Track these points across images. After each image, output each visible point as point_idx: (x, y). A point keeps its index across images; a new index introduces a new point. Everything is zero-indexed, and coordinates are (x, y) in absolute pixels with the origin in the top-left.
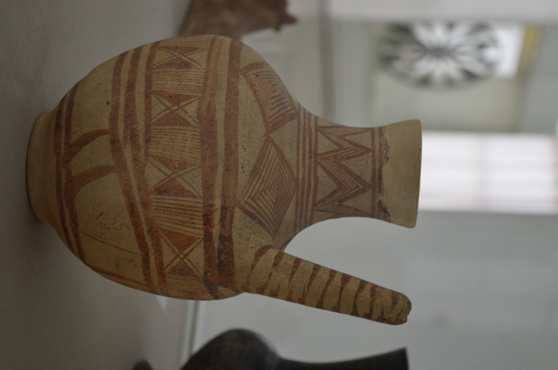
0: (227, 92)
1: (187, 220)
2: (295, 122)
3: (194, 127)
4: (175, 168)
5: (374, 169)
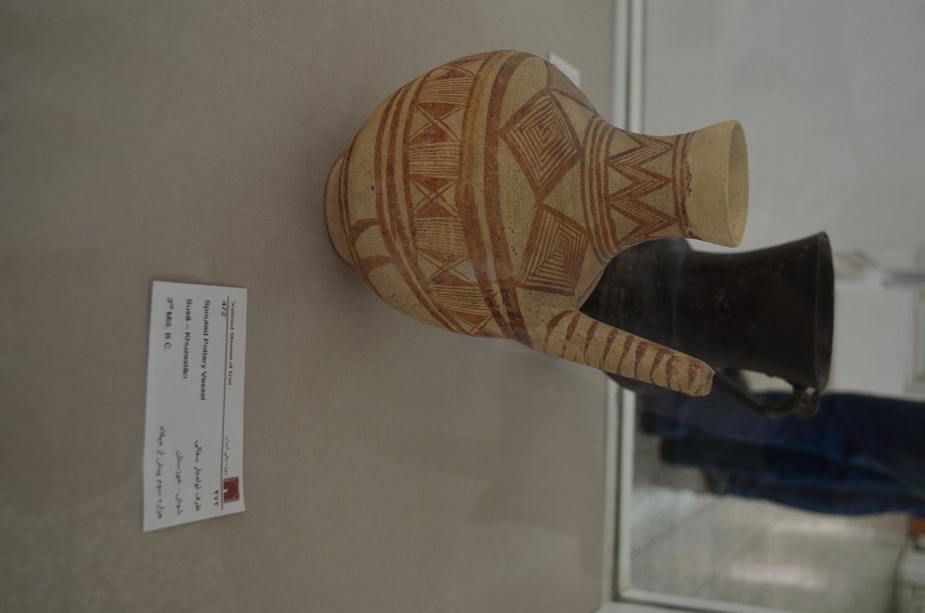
0: (485, 169)
1: (471, 304)
2: (576, 168)
4: (445, 260)
5: (676, 203)
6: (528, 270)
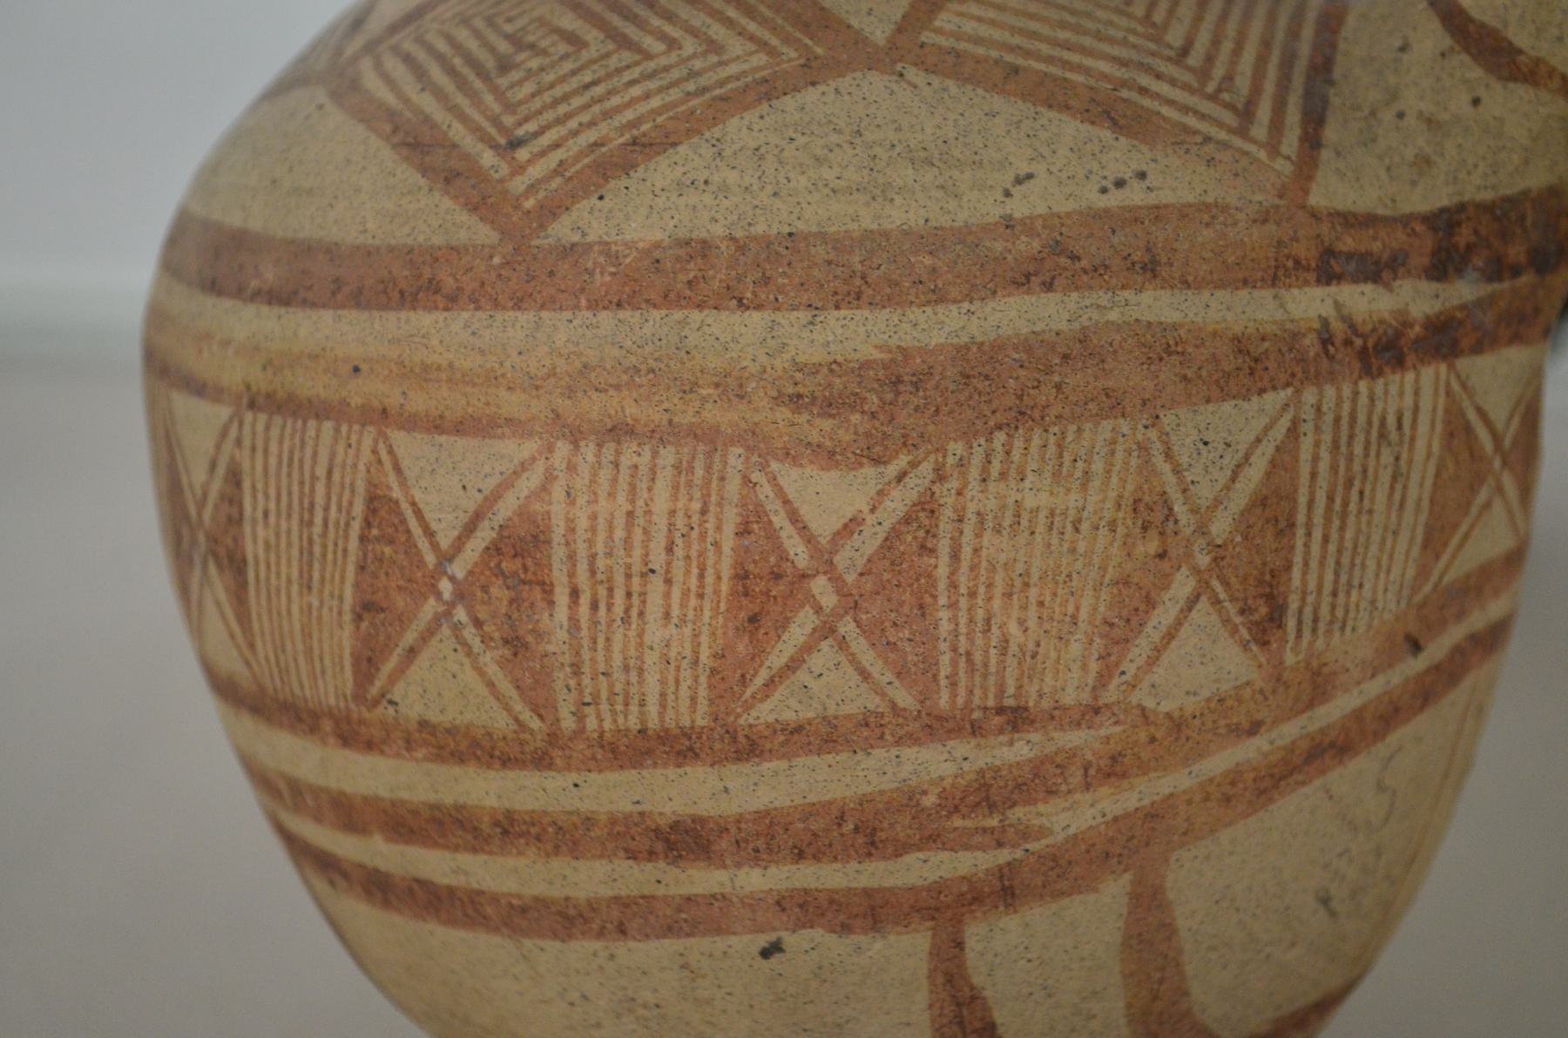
0: (700, 306)
1: (1387, 457)
3: (940, 476)
4: (1162, 556)
6: (1223, 135)
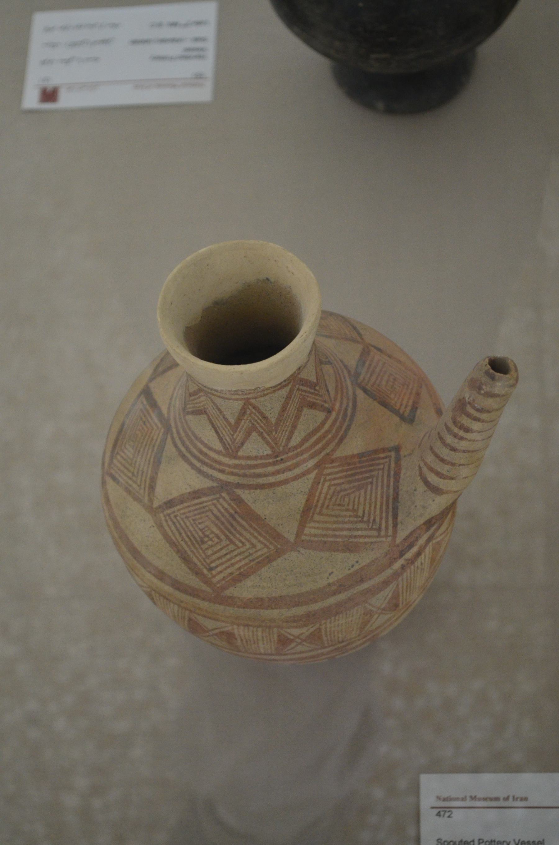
2: (245, 495)
3: (320, 625)
6: (375, 540)
